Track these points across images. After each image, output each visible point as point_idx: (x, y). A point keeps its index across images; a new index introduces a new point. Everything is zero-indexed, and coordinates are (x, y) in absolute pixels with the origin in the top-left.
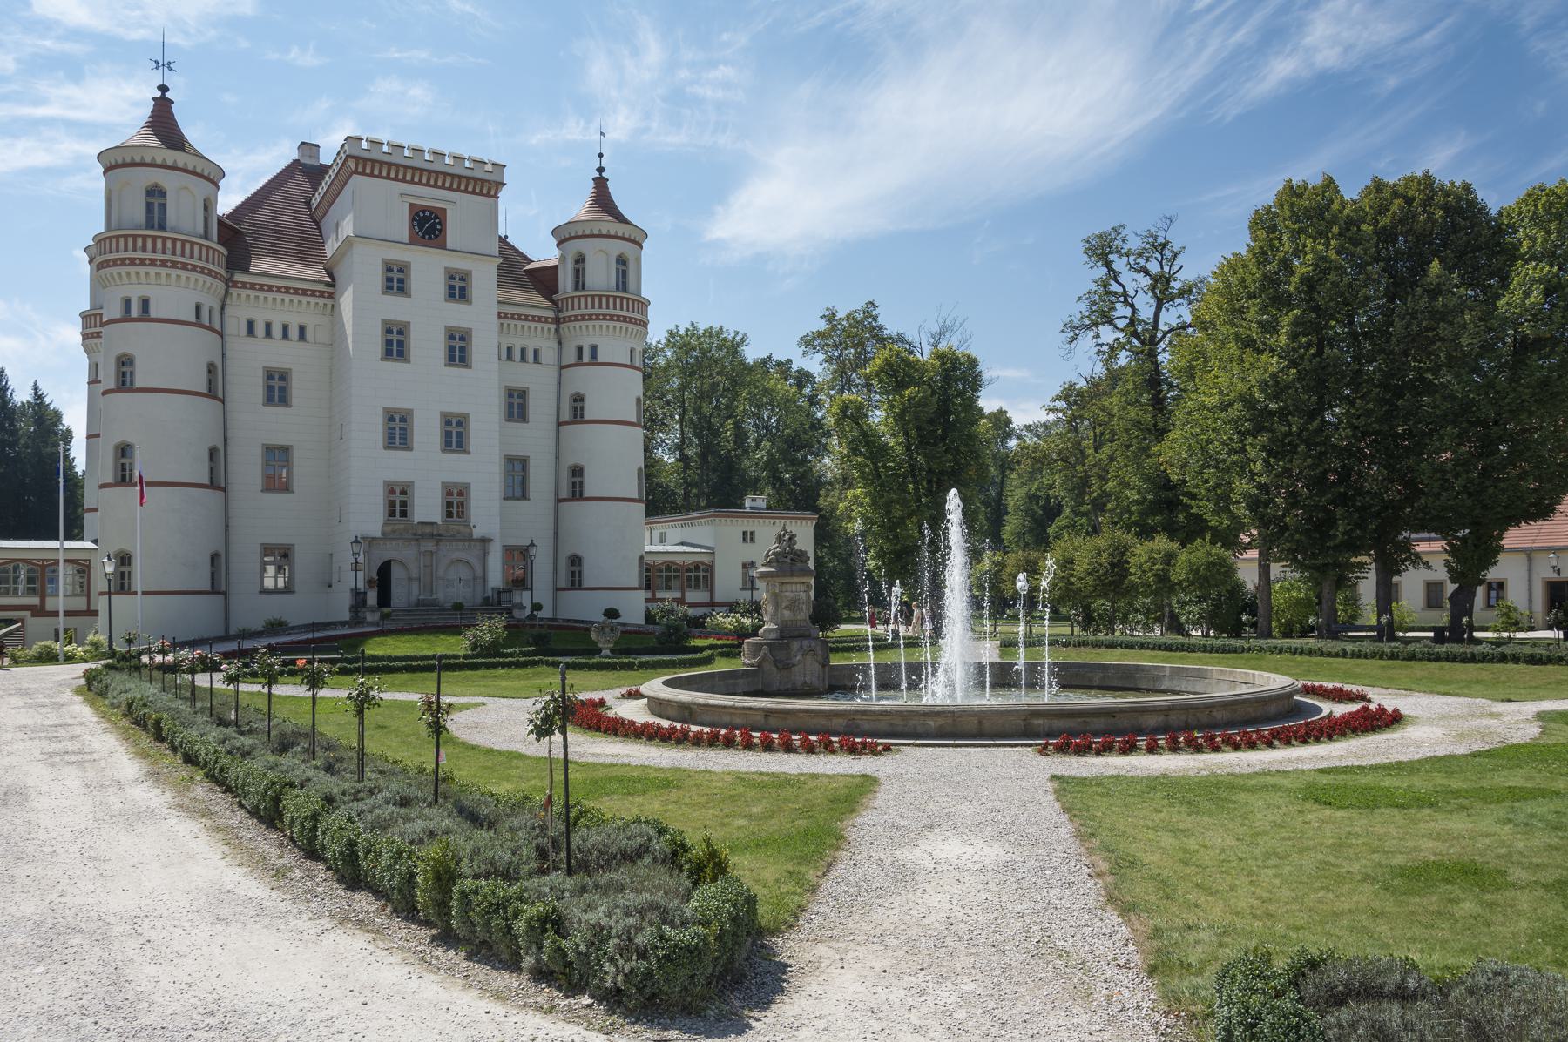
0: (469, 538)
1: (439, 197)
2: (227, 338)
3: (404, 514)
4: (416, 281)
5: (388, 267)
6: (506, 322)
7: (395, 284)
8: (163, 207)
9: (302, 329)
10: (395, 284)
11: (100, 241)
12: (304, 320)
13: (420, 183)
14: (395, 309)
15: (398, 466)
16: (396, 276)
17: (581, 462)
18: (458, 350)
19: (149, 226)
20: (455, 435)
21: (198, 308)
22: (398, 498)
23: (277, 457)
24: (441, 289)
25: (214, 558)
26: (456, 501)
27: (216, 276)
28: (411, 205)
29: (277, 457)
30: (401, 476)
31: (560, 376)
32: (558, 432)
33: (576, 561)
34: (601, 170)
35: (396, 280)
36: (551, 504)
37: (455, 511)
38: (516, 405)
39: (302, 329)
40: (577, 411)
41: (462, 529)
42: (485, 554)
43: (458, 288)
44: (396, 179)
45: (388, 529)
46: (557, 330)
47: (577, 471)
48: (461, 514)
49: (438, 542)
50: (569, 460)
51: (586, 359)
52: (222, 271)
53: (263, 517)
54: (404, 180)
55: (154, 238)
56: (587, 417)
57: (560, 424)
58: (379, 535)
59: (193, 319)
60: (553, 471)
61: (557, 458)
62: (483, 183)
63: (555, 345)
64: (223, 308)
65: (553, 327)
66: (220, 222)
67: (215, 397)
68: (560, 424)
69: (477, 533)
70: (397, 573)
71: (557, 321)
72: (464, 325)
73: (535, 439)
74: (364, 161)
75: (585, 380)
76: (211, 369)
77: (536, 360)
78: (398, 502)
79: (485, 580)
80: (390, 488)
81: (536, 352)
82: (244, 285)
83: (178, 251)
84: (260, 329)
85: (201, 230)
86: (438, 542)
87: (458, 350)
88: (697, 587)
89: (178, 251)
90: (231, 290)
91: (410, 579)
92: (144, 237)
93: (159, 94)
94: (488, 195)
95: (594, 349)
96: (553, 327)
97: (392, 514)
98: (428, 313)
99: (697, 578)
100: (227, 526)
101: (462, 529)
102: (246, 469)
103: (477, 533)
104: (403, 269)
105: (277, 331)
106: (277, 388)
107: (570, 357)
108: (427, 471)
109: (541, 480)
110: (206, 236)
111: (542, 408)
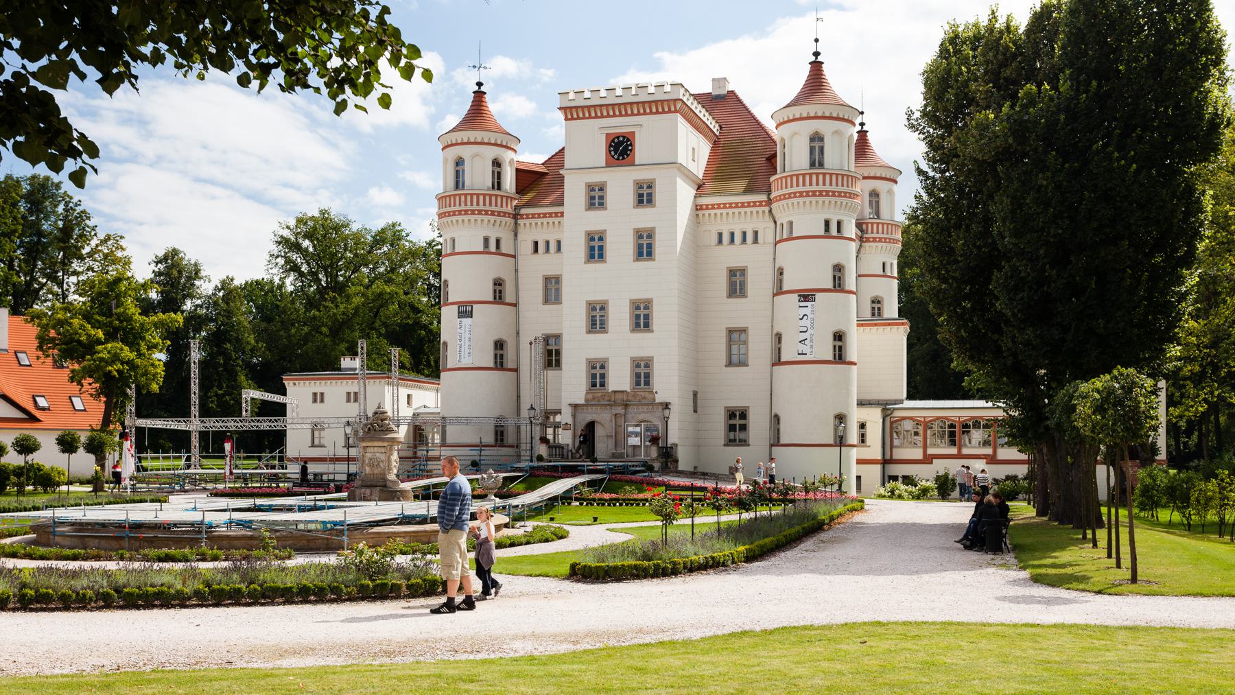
0: (653, 403)
2: (520, 258)
3: (603, 385)
4: (611, 196)
5: (591, 188)
7: (597, 201)
10: (597, 201)
11: (441, 199)
14: (596, 220)
15: (598, 346)
16: (597, 194)
17: (781, 331)
18: (644, 248)
20: (642, 319)
21: (486, 240)
24: (631, 197)
26: (642, 373)
28: (608, 135)
34: (816, 54)
41: (647, 394)
43: (644, 196)
44: (596, 117)
45: (590, 396)
46: (770, 211)
48: (647, 383)
49: (626, 406)
54: (602, 117)
56: (785, 288)
58: (582, 402)
65: (767, 209)
69: (659, 399)
70: (599, 432)
72: (648, 225)
73: (751, 311)
76: (498, 283)
77: (756, 240)
78: (597, 374)
80: (592, 364)
81: (756, 233)
86: (626, 406)
87: (644, 248)
93: (476, 88)
95: (791, 224)
96: (767, 209)
97: (594, 385)
98: (620, 220)
101: (647, 394)
108: (619, 348)
109: (759, 349)
111: (760, 283)
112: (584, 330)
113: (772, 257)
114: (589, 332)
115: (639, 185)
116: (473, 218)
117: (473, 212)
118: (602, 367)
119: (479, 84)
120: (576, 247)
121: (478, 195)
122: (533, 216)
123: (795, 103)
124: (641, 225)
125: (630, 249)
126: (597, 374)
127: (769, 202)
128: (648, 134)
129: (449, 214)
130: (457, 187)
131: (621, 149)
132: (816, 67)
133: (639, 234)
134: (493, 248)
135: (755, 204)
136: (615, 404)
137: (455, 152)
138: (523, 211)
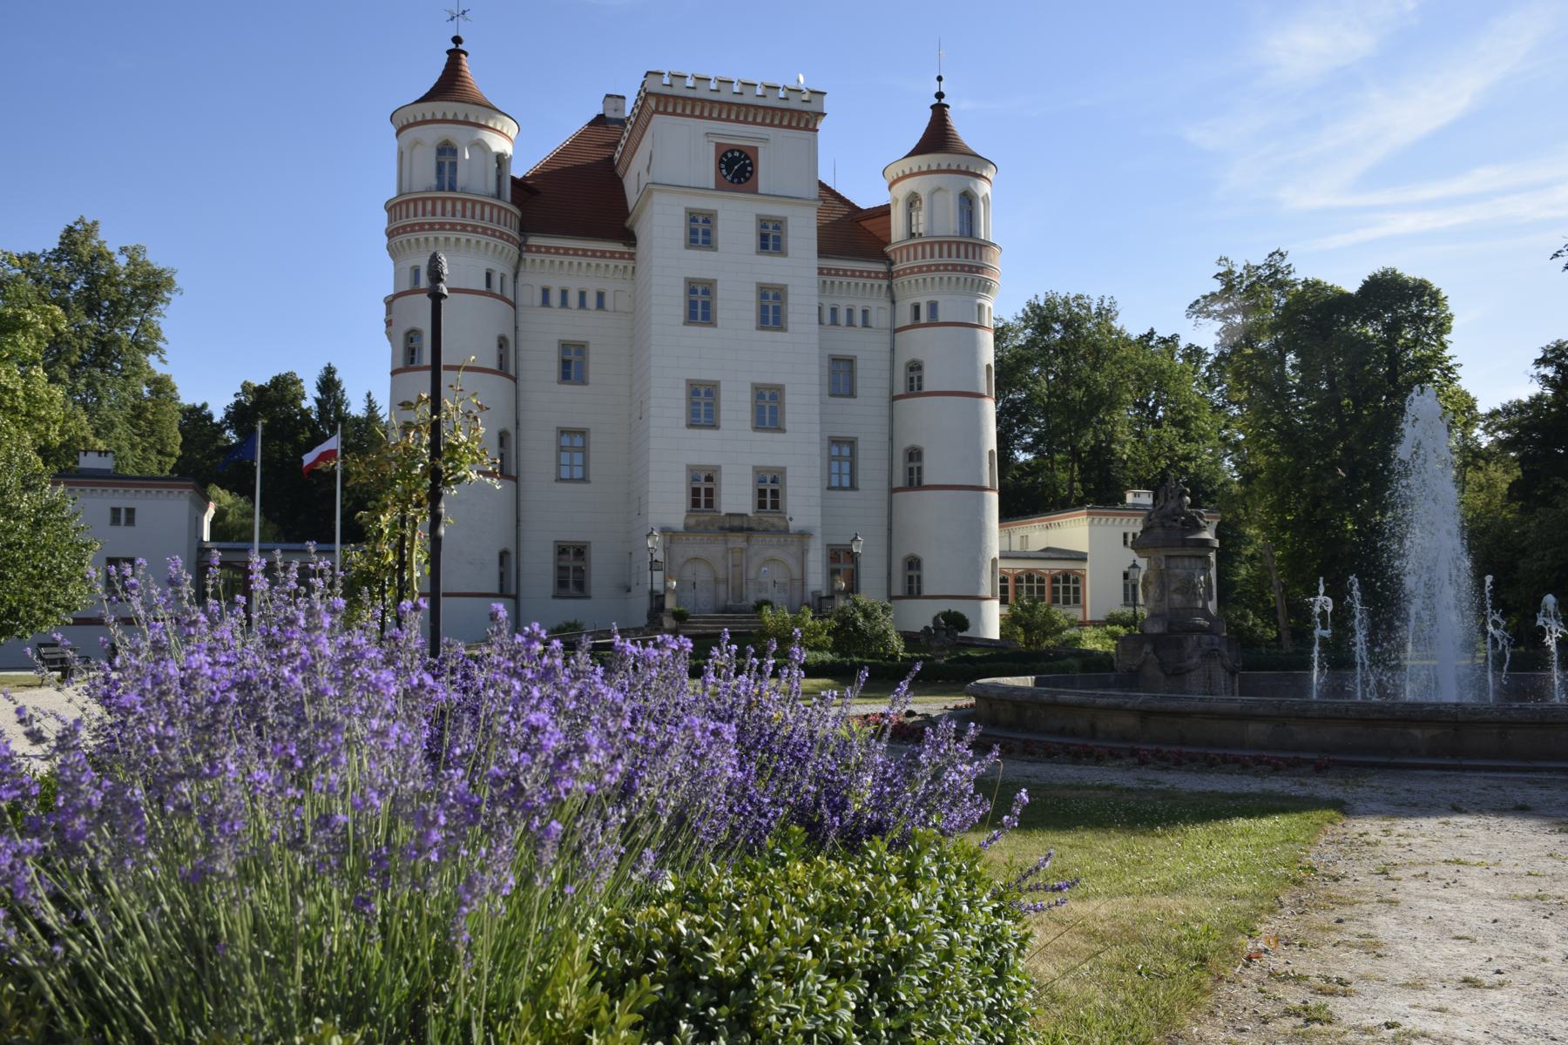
0: (786, 531)
1: (752, 132)
2: (520, 310)
3: (709, 504)
4: (723, 232)
5: (692, 216)
6: (828, 279)
7: (700, 237)
8: (454, 166)
9: (600, 296)
10: (700, 237)
11: (392, 208)
12: (602, 286)
13: (728, 119)
14: (700, 264)
15: (704, 448)
17: (918, 443)
19: (440, 188)
20: (768, 409)
21: (488, 276)
22: (703, 486)
23: (574, 439)
24: (753, 239)
25: (503, 555)
27: (509, 239)
28: (718, 145)
29: (574, 439)
30: (708, 460)
31: (893, 341)
32: (891, 408)
33: (913, 564)
34: (940, 95)
35: (701, 232)
36: (885, 495)
37: (769, 499)
38: (841, 376)
39: (600, 296)
40: (914, 381)
42: (804, 553)
44: (701, 116)
45: (692, 521)
46: (890, 287)
47: (914, 455)
48: (775, 505)
50: (905, 441)
51: (924, 319)
52: (515, 234)
53: (559, 513)
54: (710, 118)
55: (444, 200)
56: (926, 388)
57: (894, 398)
59: (483, 288)
60: (885, 454)
61: (891, 439)
62: (800, 116)
63: (888, 305)
64: (516, 276)
65: (885, 283)
66: (513, 178)
67: (506, 375)
68: (894, 398)
69: (793, 526)
71: (889, 275)
73: (862, 416)
74: (664, 99)
75: (920, 343)
76: (502, 342)
77: (866, 324)
79: (803, 583)
81: (865, 312)
82: (538, 249)
83: (469, 213)
84: (555, 298)
85: (492, 188)
87: (771, 309)
88: (1066, 602)
89: (469, 213)
90: (528, 257)
91: (716, 581)
92: (434, 200)
94: (806, 128)
95: (933, 306)
96: (885, 283)
97: (696, 503)
98: (737, 268)
99: (1066, 590)
100: (518, 521)
101: (776, 521)
102: (539, 454)
103: (794, 526)
104: (709, 218)
105: (573, 299)
106: (572, 365)
107: (905, 317)
108: (736, 455)
110: (499, 195)
111: (872, 379)
112: (683, 422)
113: (888, 347)
114: (691, 425)
115: (763, 222)
116: (474, 238)
117: (475, 230)
118: (709, 479)
119: (457, 40)
120: (668, 303)
121: (483, 204)
122: (548, 250)
123: (916, 152)
124: (767, 279)
125: (751, 313)
126: (703, 492)
127: (889, 275)
128: (775, 153)
129: (413, 228)
130: (440, 188)
131: (737, 169)
132: (939, 111)
133: (764, 291)
134: (498, 291)
135: (869, 275)
136: (732, 529)
137: (432, 135)
138: (534, 241)
